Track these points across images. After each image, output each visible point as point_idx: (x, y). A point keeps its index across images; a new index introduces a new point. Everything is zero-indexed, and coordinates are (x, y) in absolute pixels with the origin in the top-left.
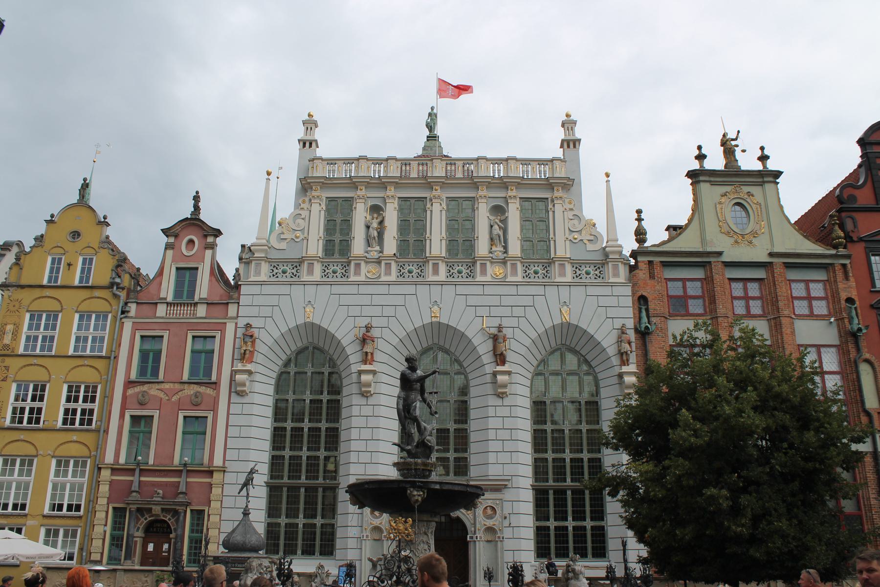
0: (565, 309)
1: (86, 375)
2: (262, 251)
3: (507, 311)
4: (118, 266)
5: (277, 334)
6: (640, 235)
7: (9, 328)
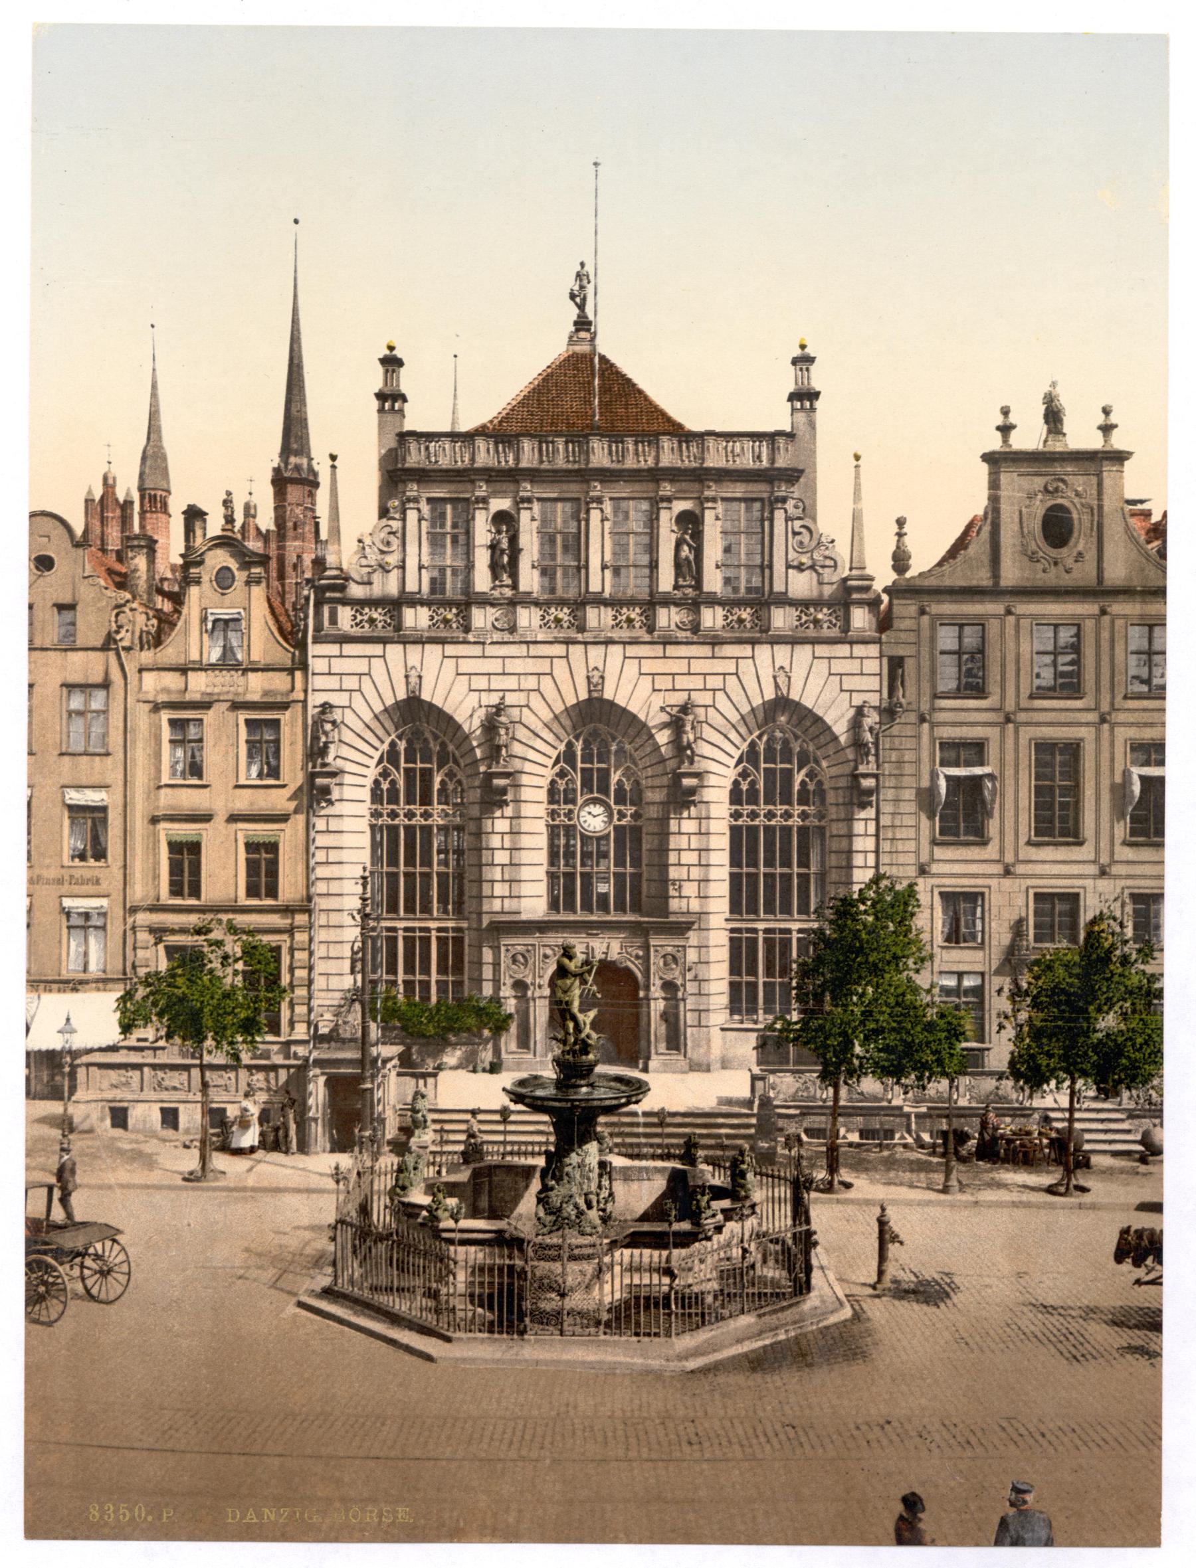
0: (782, 680)
3: (697, 682)
6: (900, 561)
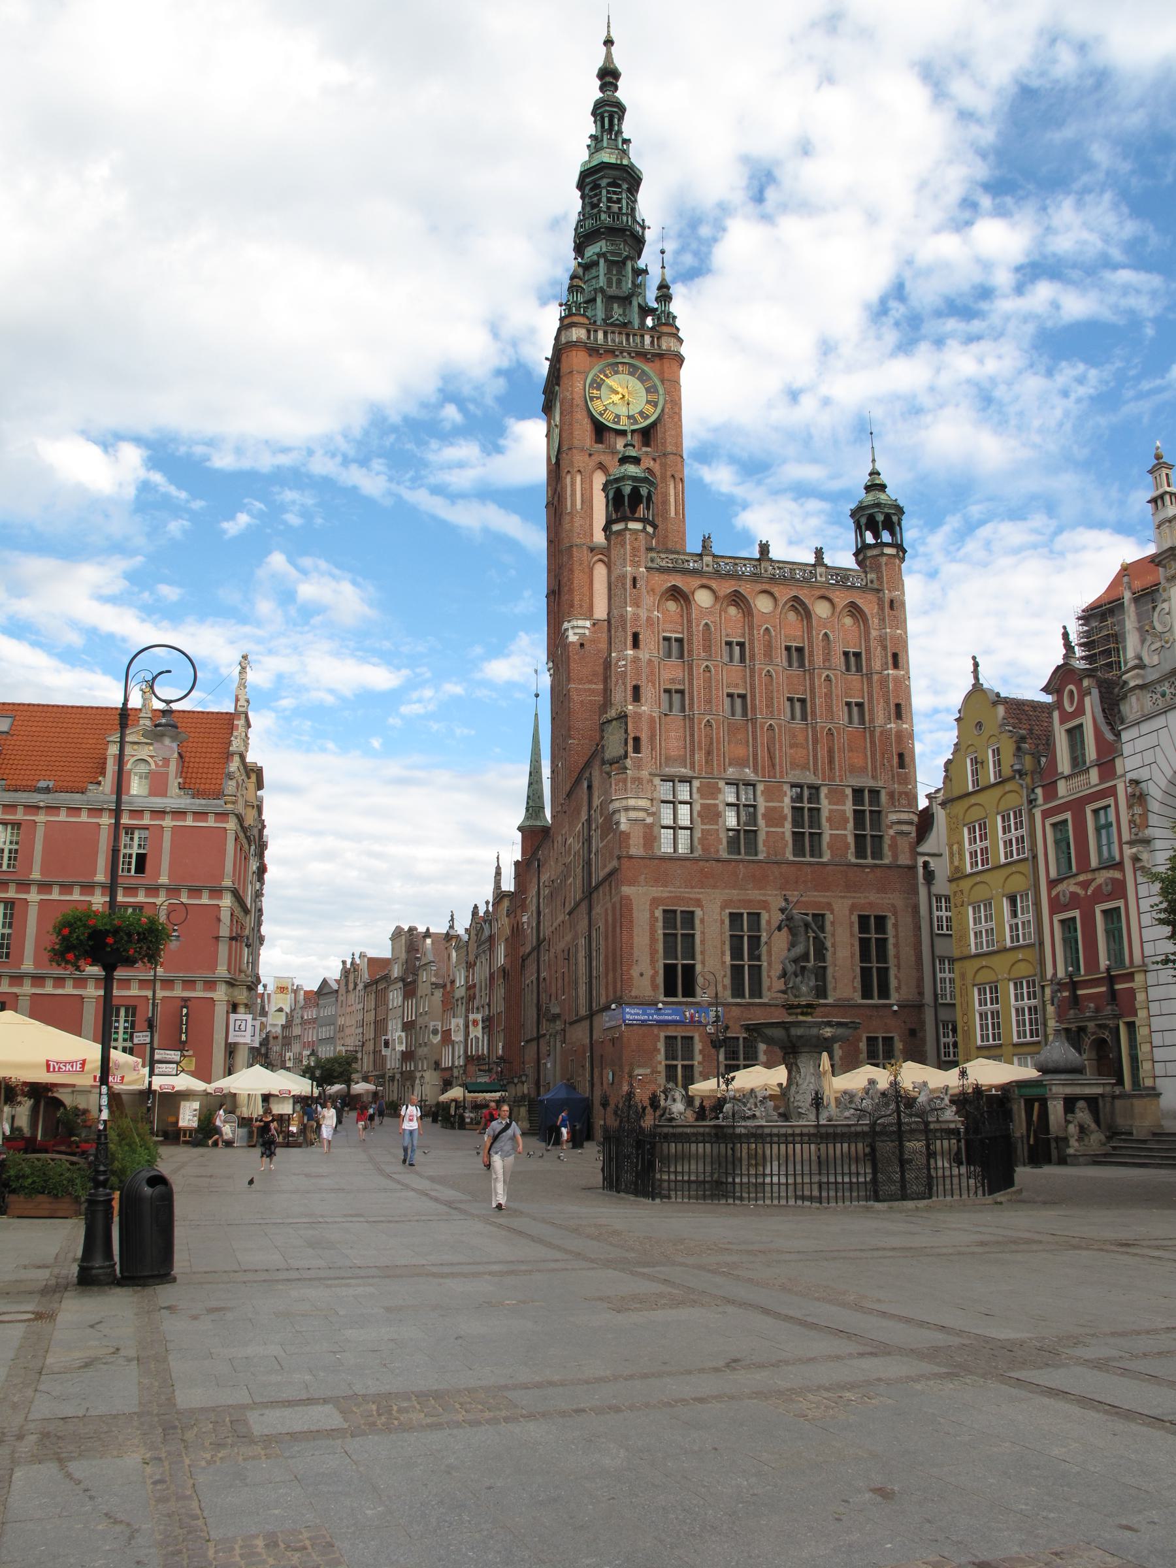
1: (1018, 883)
2: (1133, 677)
4: (1019, 749)
5: (1163, 783)
7: (955, 847)
